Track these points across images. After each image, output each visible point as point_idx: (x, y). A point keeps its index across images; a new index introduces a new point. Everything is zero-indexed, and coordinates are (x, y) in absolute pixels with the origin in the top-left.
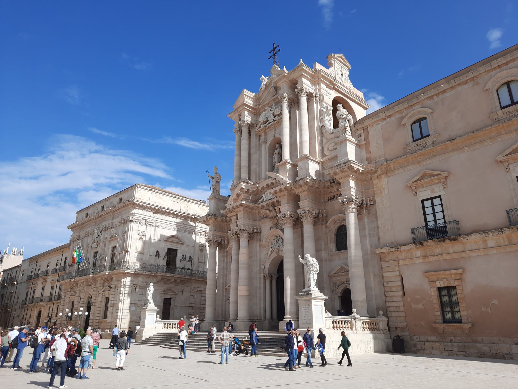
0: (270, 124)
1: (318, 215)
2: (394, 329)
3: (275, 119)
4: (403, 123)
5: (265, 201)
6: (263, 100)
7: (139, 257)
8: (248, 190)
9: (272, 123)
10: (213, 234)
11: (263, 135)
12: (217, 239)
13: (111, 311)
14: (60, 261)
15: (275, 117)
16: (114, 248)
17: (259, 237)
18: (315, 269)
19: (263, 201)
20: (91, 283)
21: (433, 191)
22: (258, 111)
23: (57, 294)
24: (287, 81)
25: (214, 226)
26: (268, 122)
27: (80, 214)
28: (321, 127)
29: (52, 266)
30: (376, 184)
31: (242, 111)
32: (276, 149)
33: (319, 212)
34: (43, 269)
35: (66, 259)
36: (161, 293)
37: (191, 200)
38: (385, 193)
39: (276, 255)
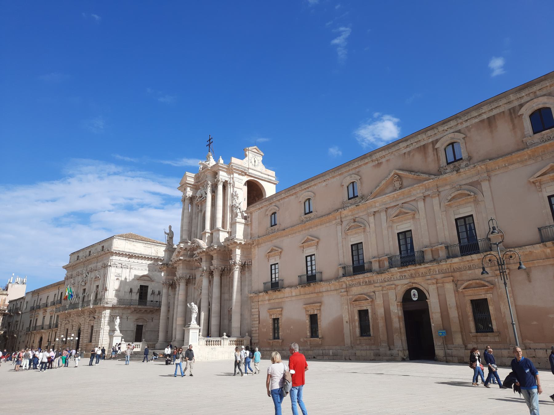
0: (204, 199)
1: (224, 270)
4: (267, 214)
5: (197, 256)
6: (201, 178)
7: (116, 294)
10: (166, 278)
13: (95, 337)
14: (57, 295)
16: (98, 286)
17: (194, 282)
18: (195, 312)
20: (80, 314)
21: (275, 260)
22: (198, 187)
23: (55, 322)
24: (211, 172)
25: (167, 272)
26: (202, 197)
27: (73, 256)
29: (51, 299)
33: (225, 267)
34: (44, 301)
35: (62, 293)
36: (134, 321)
37: (160, 245)
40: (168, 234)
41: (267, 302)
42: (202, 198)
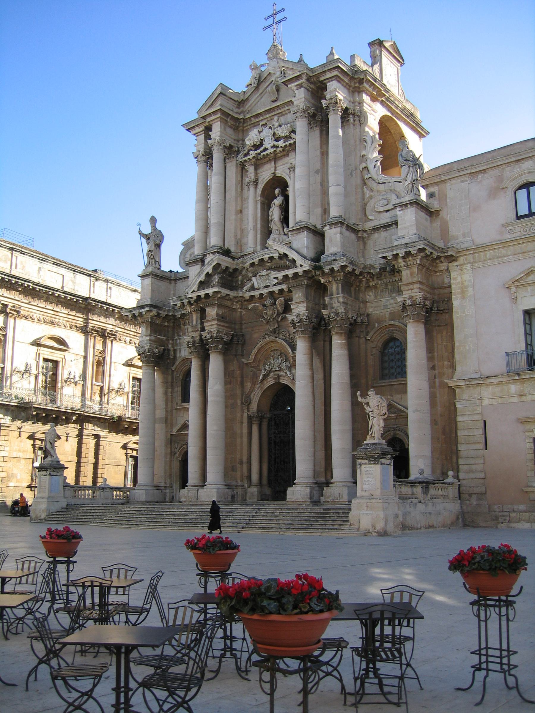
0: (267, 152)
2: (467, 496)
3: (276, 143)
6: (251, 104)
8: (227, 267)
9: (272, 150)
11: (251, 169)
12: (157, 348)
15: (277, 140)
19: (252, 288)
26: (263, 148)
28: (363, 169)
30: (455, 279)
31: (214, 121)
32: (275, 197)
38: (469, 294)
39: (272, 382)
40: (148, 238)
41: (515, 399)
42: (261, 149)
